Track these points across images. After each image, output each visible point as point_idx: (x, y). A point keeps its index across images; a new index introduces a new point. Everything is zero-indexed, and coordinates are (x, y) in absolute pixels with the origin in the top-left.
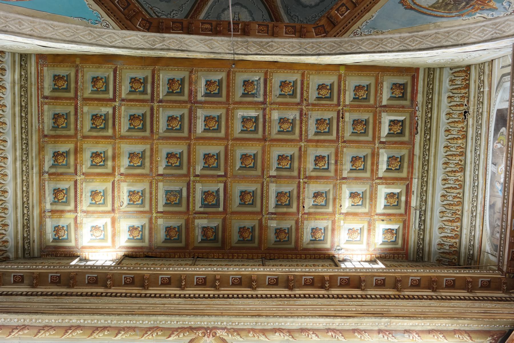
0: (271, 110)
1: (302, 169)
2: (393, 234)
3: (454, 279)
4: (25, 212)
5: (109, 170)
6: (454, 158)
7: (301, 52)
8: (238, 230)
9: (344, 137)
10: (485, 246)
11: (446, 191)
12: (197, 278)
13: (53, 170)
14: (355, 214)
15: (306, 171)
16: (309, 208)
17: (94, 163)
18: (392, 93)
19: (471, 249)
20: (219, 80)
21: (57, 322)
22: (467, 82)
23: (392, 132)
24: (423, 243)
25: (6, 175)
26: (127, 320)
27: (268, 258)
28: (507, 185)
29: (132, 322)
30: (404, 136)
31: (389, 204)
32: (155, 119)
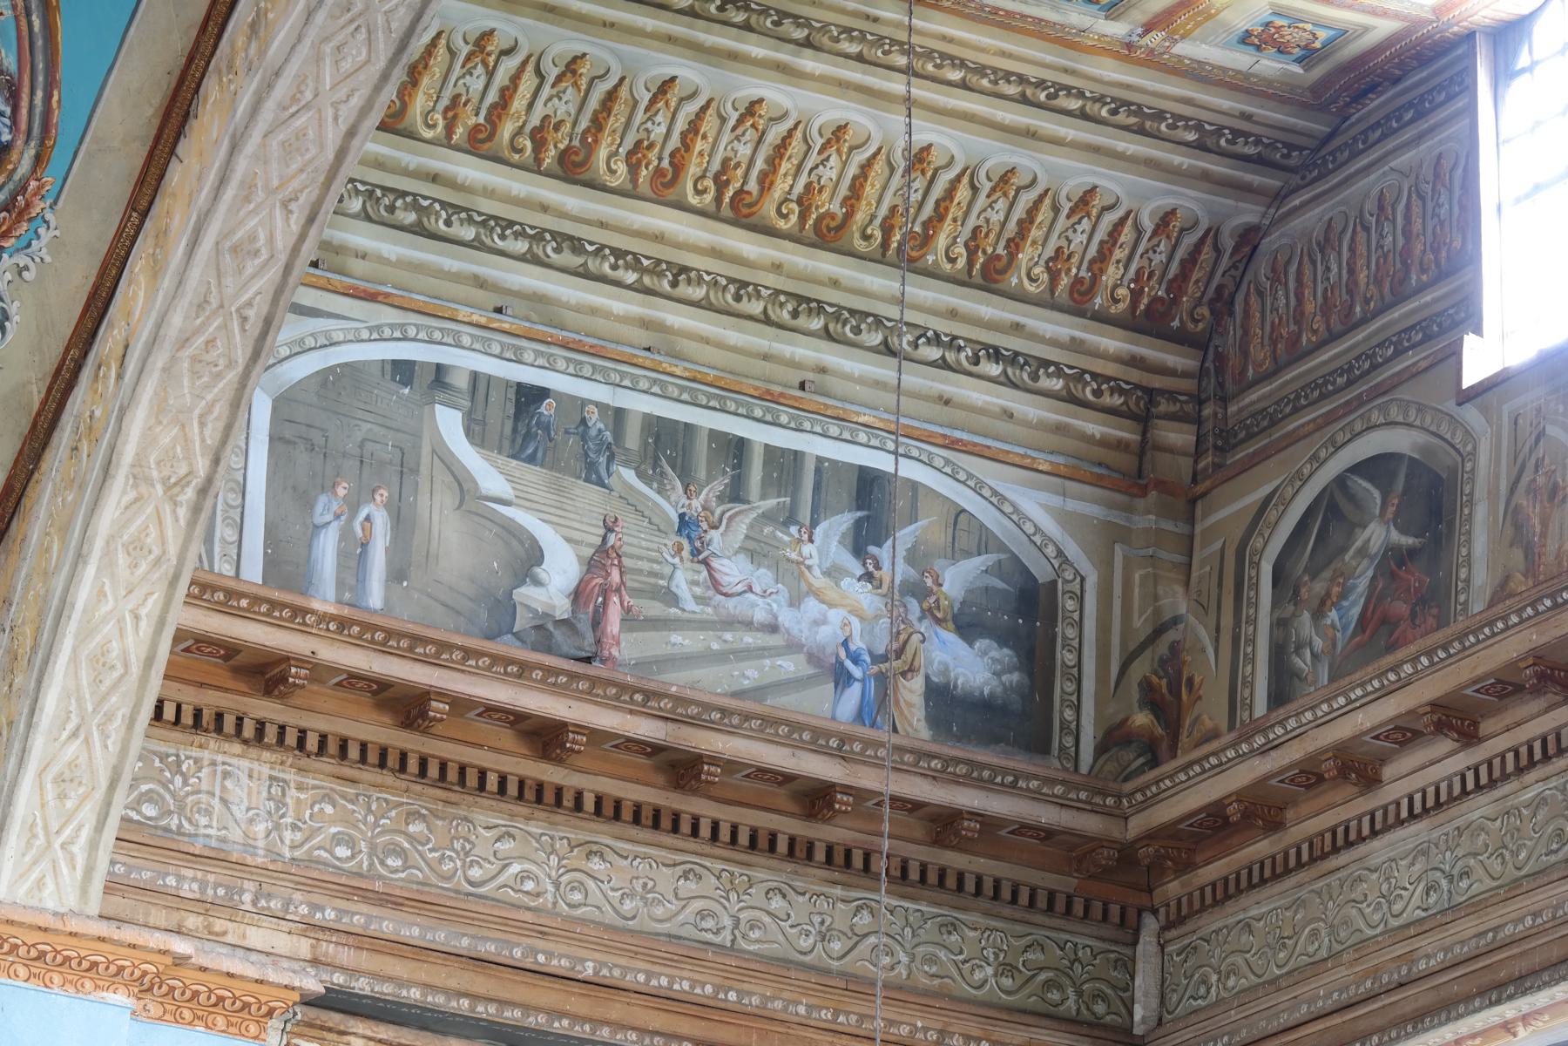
4: (1075, 104)
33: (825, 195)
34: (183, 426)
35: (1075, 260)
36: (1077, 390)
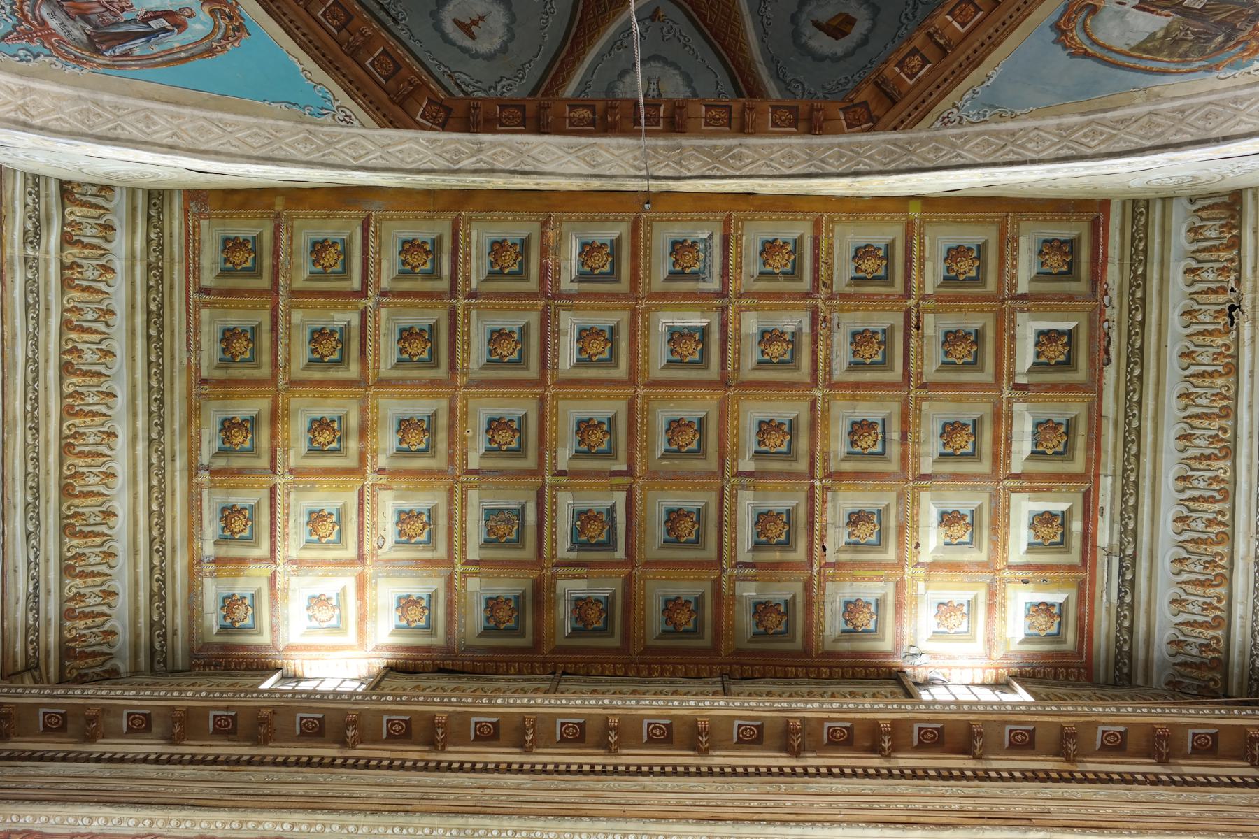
0: (740, 310)
1: (818, 455)
2: (1051, 616)
3: (1214, 731)
4: (156, 562)
5: (352, 462)
6: (1206, 423)
7: (812, 170)
8: (662, 606)
9: (922, 375)
11: (1187, 507)
12: (563, 724)
13: (221, 463)
14: (954, 567)
15: (828, 460)
16: (838, 551)
17: (315, 445)
18: (1043, 264)
20: (612, 241)
21: (228, 827)
22: (1235, 232)
23: (1043, 359)
25: (113, 475)
26: (394, 826)
27: (738, 676)
29: (405, 831)
30: (1076, 370)
31: (1040, 541)
32: (459, 337)
33: (82, 482)
34: (54, 110)
35: (82, 604)
36: (31, 632)
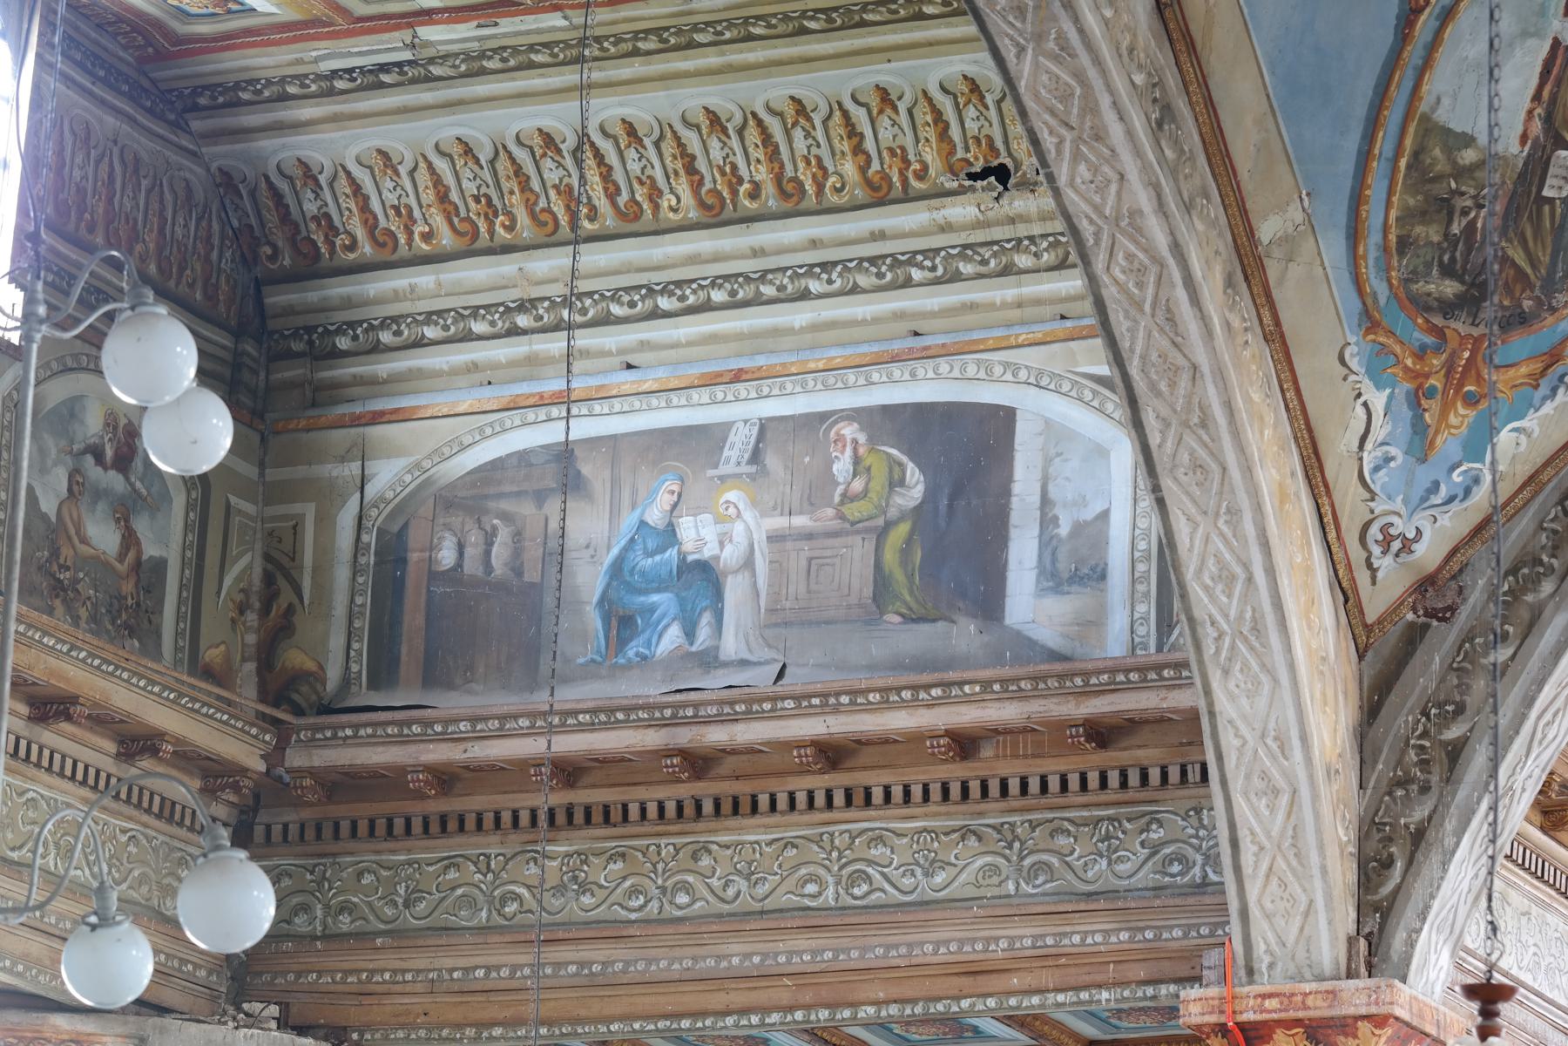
6: (759, 154)
10: (393, 452)
19: (355, 338)
24: (269, 100)
28: (620, 716)
